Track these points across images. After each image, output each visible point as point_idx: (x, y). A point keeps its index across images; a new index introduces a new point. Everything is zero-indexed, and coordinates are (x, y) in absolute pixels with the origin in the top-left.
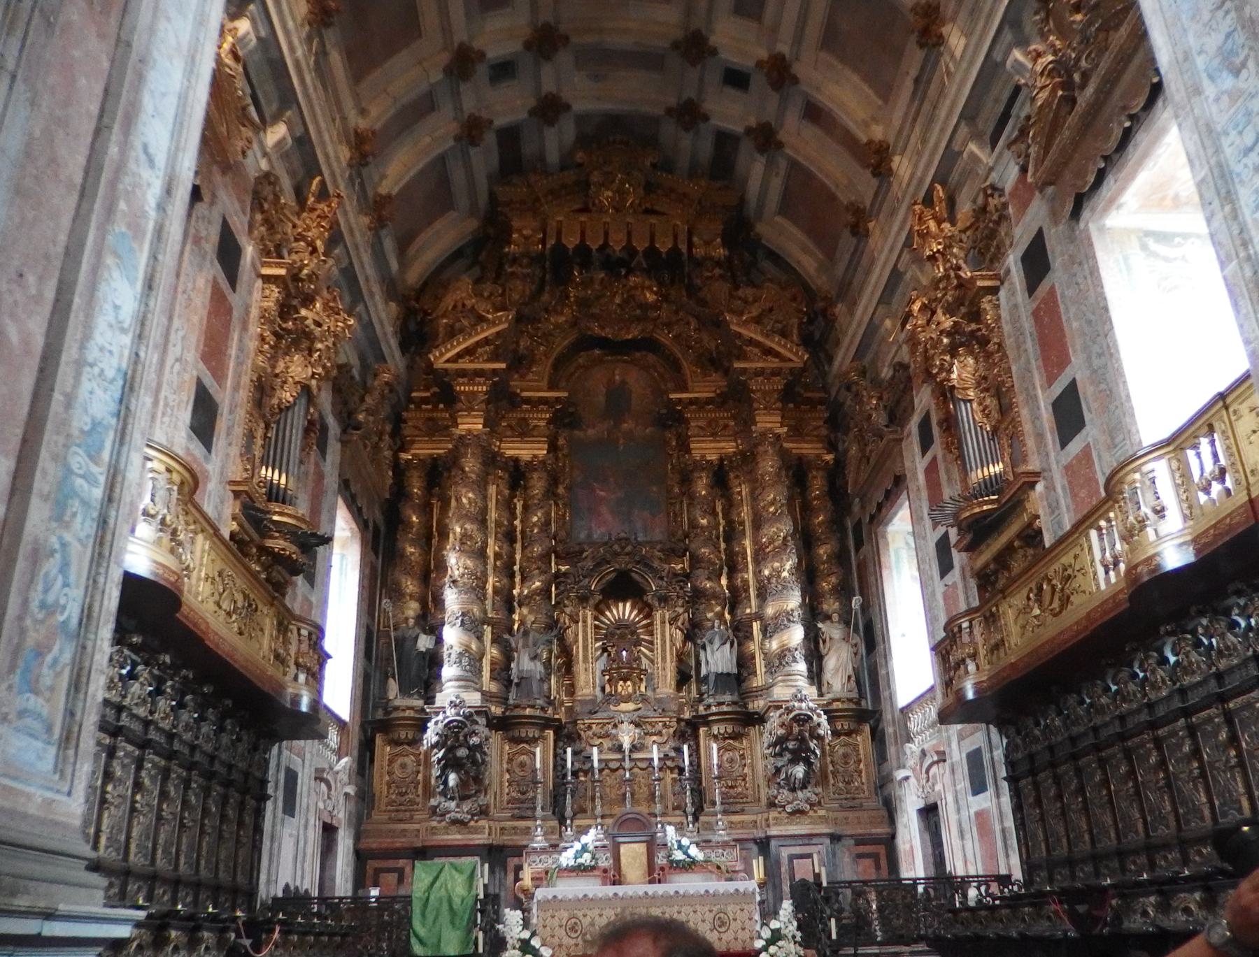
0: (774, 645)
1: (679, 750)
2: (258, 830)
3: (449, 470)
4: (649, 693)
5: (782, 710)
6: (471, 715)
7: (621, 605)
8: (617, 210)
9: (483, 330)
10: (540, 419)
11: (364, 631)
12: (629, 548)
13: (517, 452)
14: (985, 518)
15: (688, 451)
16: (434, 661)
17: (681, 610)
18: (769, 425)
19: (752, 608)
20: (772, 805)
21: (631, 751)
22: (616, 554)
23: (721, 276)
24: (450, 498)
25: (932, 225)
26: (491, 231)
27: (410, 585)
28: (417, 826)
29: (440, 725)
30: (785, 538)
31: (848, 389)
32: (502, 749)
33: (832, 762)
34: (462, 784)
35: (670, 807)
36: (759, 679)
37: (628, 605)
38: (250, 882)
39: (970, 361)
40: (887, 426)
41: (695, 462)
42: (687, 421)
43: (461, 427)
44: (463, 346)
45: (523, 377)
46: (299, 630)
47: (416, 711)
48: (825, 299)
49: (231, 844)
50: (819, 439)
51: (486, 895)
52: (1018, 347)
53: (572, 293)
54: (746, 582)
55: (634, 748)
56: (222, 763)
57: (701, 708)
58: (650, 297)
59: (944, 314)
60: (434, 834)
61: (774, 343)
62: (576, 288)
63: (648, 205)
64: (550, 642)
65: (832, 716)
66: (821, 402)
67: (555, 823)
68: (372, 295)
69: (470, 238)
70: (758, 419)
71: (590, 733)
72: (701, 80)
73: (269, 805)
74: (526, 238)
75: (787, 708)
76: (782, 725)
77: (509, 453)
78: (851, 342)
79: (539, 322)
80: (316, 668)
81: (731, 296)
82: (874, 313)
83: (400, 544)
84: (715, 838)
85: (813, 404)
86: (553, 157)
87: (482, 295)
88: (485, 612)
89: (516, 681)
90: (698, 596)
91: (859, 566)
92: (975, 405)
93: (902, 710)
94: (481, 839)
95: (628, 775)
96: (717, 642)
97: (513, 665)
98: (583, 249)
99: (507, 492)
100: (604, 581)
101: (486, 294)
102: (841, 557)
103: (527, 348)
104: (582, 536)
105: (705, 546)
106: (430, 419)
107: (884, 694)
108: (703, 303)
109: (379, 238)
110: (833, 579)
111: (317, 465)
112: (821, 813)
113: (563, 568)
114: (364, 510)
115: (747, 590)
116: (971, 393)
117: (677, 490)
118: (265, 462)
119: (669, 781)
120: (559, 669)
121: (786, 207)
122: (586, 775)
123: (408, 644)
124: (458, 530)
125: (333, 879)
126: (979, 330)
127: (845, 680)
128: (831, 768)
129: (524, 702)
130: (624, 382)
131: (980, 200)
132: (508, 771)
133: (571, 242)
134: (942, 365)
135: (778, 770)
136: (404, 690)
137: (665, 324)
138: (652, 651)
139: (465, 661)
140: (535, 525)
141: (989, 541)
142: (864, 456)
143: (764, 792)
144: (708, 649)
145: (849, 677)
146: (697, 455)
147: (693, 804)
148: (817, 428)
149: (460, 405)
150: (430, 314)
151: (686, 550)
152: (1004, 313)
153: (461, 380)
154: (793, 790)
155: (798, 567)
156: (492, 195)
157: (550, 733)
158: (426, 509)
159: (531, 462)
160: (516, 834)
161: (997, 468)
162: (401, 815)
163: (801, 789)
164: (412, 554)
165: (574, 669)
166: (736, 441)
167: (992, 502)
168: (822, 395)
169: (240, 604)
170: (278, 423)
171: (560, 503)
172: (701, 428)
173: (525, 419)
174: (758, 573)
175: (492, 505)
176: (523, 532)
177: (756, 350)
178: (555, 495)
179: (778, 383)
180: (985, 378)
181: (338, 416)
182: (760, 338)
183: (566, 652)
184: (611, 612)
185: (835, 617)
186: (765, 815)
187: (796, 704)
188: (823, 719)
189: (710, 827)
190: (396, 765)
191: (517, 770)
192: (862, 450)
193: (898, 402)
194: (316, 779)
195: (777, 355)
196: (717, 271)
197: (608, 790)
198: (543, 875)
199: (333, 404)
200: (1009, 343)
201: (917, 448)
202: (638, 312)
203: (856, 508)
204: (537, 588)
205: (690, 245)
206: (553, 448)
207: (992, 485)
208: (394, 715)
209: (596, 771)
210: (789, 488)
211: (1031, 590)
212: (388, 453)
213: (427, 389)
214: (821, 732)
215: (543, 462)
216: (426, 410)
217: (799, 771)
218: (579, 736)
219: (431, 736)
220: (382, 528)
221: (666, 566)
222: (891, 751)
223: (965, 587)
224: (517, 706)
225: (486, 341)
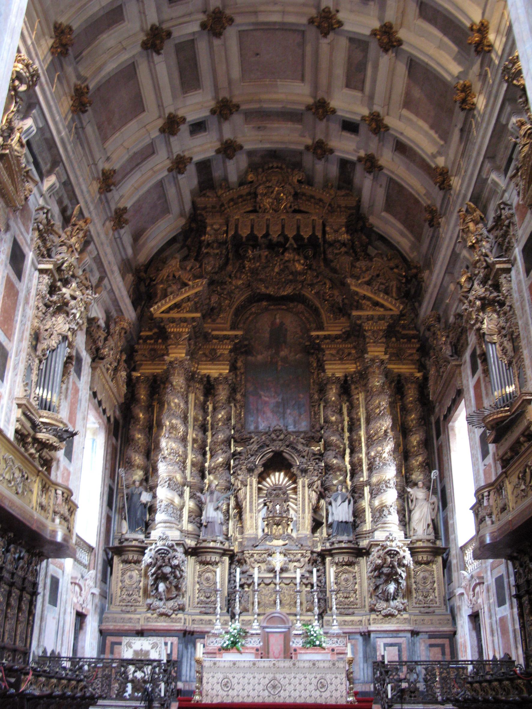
0: (377, 503)
1: (311, 572)
2: (31, 613)
3: (164, 383)
4: (294, 535)
5: (379, 547)
6: (173, 546)
7: (277, 474)
8: (276, 211)
9: (186, 291)
10: (225, 349)
11: (107, 489)
12: (282, 437)
14: (503, 422)
15: (324, 371)
16: (151, 509)
17: (316, 478)
18: (376, 354)
19: (364, 477)
20: (373, 610)
21: (280, 573)
22: (273, 440)
23: (346, 253)
24: (164, 402)
25: (471, 225)
26: (194, 225)
27: (138, 459)
28: (138, 616)
29: (153, 552)
30: (386, 431)
31: (429, 330)
33: (415, 582)
34: (168, 590)
35: (304, 610)
36: (367, 526)
37: (282, 474)
38: (25, 645)
39: (495, 316)
40: (451, 356)
41: (328, 378)
42: (323, 350)
43: (171, 355)
44: (173, 302)
45: (214, 321)
46: (56, 490)
47: (140, 542)
48: (416, 267)
49: (13, 622)
50: (413, 362)
51: (168, 661)
52: (522, 309)
53: (247, 264)
54: (360, 460)
55: (282, 570)
56: (8, 571)
57: (328, 544)
58: (299, 267)
59: (478, 284)
60: (149, 621)
61: (380, 298)
62: (250, 261)
63: (296, 207)
64: (229, 499)
65: (413, 552)
66: (414, 337)
67: (228, 618)
68: (112, 272)
69: (180, 230)
70: (369, 349)
71: (252, 559)
72: (327, 127)
73: (40, 598)
74: (216, 230)
75: (382, 546)
76: (379, 557)
78: (431, 297)
79: (225, 283)
80: (67, 514)
81: (353, 266)
82: (443, 279)
83: (131, 432)
84: (331, 631)
85: (409, 338)
86: (233, 178)
87: (186, 269)
88: (186, 478)
89: (205, 524)
90: (328, 468)
91: (438, 449)
92: (497, 346)
94: (179, 626)
95: (278, 588)
96: (339, 500)
97: (204, 513)
98: (252, 237)
99: (202, 398)
100: (265, 458)
101: (188, 268)
102: (427, 443)
103: (216, 302)
104: (252, 428)
105: (334, 435)
106: (152, 350)
107: (452, 537)
108: (334, 271)
109: (119, 234)
110: (420, 459)
111: (74, 383)
112: (406, 616)
113: (239, 449)
114: (107, 410)
115: (361, 465)
116: (495, 338)
117: (316, 397)
119: (304, 593)
120: (235, 516)
121: (389, 207)
122: (249, 587)
123: (135, 498)
124: (168, 423)
125: (83, 648)
126: (498, 296)
127: (425, 527)
128: (414, 586)
129: (209, 538)
130: (282, 324)
131: (499, 212)
132: (198, 583)
133: (245, 232)
134: (477, 318)
135: (377, 587)
136: (132, 528)
137: (308, 285)
138: (296, 505)
139: (170, 510)
140: (219, 420)
141: (506, 436)
142: (439, 375)
143: (368, 600)
144: (333, 504)
145: (428, 525)
146: (329, 373)
147: (319, 607)
148: (411, 355)
149: (170, 342)
150: (154, 280)
151: (321, 438)
152: (514, 285)
153: (171, 325)
154: (387, 600)
155: (395, 450)
157: (226, 559)
158: (149, 408)
159: (218, 378)
160: (202, 624)
161: (510, 389)
162: (129, 609)
163: (393, 600)
164: (139, 439)
165: (243, 517)
166: (355, 363)
167: (506, 411)
168: (415, 332)
169: (16, 475)
170: (47, 359)
171: (238, 405)
172: (332, 355)
173: (214, 350)
174: (368, 454)
175: (191, 406)
176: (212, 425)
177: (368, 303)
178: (235, 400)
179: (383, 325)
180: (503, 328)
181: (89, 350)
182: (369, 295)
183: (239, 506)
184: (270, 478)
185: (420, 484)
186: (368, 617)
187: (388, 543)
188: (408, 554)
189: (329, 624)
190: (126, 577)
191: (204, 583)
192: (438, 371)
193: (458, 340)
194: (72, 583)
195: (382, 306)
196: (343, 249)
197: (263, 597)
198: (217, 651)
199: (86, 343)
200: (517, 305)
201: (469, 372)
202: (291, 277)
203: (437, 410)
204: (220, 463)
205: (324, 232)
206: (233, 368)
207: (508, 400)
208: (125, 544)
209: (256, 584)
210: (390, 396)
211: (520, 472)
212: (124, 374)
213: (150, 330)
214: (405, 562)
215: (226, 378)
216: (150, 344)
217: (392, 587)
218: (245, 561)
219: (147, 559)
220: (121, 422)
221: (307, 449)
222: (455, 575)
223: (495, 466)
224: (204, 541)
225: (188, 299)
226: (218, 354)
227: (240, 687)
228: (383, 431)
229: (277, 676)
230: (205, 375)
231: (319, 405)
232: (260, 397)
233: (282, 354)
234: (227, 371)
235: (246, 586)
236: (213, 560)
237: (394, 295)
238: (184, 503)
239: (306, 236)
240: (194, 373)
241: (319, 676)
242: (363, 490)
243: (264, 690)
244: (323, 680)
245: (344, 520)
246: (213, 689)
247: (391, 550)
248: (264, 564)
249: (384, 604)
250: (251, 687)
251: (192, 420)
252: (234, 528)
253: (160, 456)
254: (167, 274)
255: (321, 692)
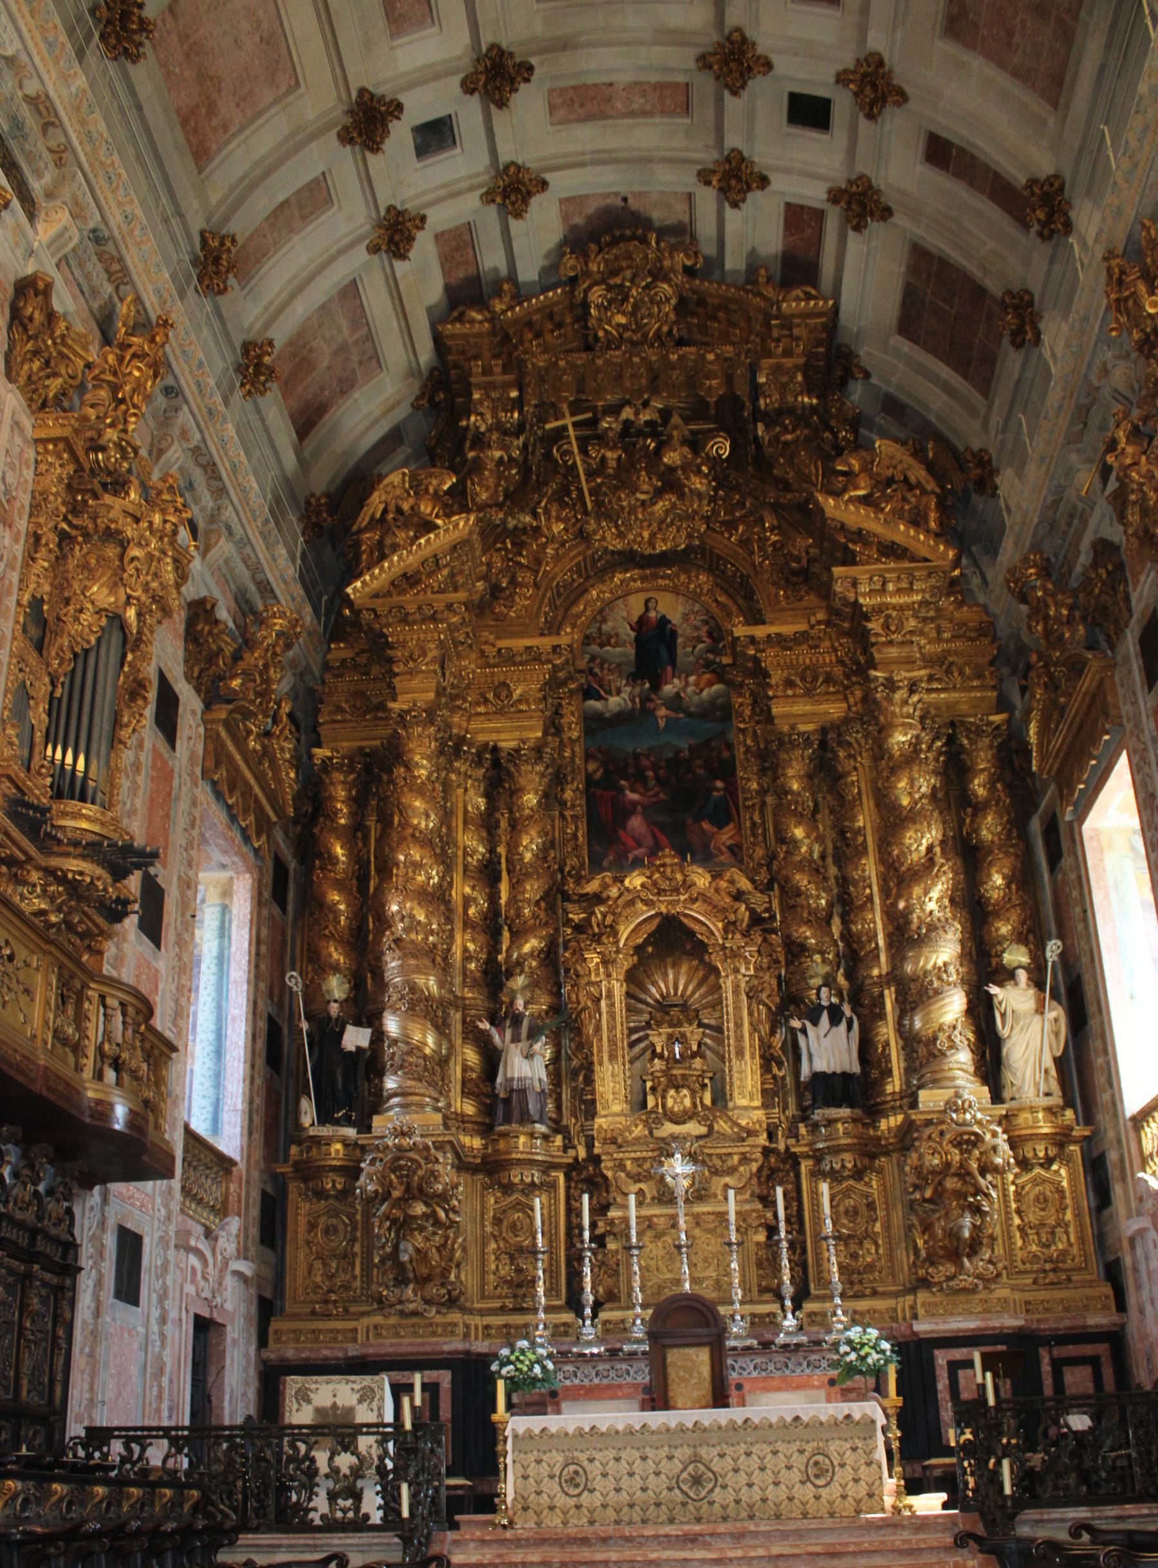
11: (262, 1024)
13: (494, 737)
30: (930, 849)
32: (483, 1202)
36: (894, 1085)
43: (400, 698)
63: (684, 334)
77: (481, 738)
86: (528, 272)
89: (502, 1095)
93: (1134, 1119)
117: (755, 786)
118: (50, 737)
132: (495, 1237)
145: (1046, 1071)
156: (438, 340)
159: (517, 750)
171: (568, 813)
185: (1022, 975)
188: (1001, 1140)
191: (508, 1235)
206: (553, 726)
214: (999, 1161)
218: (605, 1178)
226: (516, 694)
227: (610, 1483)
228: (923, 848)
229: (703, 1452)
230: (486, 744)
231: (763, 804)
232: (621, 790)
233: (668, 689)
234: (539, 734)
235: (608, 1239)
236: (528, 1180)
237: (933, 525)
238: (451, 1047)
239: (712, 400)
240: (462, 740)
241: (809, 1448)
242: (882, 995)
243: (670, 1489)
244: (819, 1458)
245: (839, 1071)
246: (539, 1493)
247: (962, 1134)
248: (651, 1183)
249: (952, 1269)
250: (637, 1482)
251: (460, 853)
252: (573, 1105)
253: (387, 939)
254: (382, 506)
255: (816, 1486)
